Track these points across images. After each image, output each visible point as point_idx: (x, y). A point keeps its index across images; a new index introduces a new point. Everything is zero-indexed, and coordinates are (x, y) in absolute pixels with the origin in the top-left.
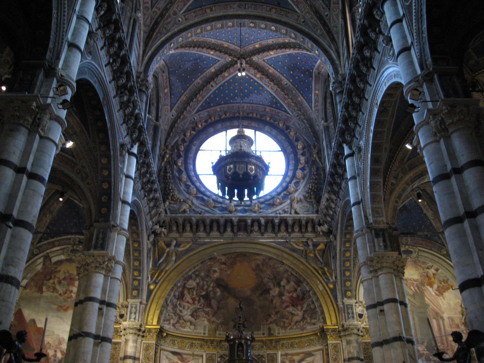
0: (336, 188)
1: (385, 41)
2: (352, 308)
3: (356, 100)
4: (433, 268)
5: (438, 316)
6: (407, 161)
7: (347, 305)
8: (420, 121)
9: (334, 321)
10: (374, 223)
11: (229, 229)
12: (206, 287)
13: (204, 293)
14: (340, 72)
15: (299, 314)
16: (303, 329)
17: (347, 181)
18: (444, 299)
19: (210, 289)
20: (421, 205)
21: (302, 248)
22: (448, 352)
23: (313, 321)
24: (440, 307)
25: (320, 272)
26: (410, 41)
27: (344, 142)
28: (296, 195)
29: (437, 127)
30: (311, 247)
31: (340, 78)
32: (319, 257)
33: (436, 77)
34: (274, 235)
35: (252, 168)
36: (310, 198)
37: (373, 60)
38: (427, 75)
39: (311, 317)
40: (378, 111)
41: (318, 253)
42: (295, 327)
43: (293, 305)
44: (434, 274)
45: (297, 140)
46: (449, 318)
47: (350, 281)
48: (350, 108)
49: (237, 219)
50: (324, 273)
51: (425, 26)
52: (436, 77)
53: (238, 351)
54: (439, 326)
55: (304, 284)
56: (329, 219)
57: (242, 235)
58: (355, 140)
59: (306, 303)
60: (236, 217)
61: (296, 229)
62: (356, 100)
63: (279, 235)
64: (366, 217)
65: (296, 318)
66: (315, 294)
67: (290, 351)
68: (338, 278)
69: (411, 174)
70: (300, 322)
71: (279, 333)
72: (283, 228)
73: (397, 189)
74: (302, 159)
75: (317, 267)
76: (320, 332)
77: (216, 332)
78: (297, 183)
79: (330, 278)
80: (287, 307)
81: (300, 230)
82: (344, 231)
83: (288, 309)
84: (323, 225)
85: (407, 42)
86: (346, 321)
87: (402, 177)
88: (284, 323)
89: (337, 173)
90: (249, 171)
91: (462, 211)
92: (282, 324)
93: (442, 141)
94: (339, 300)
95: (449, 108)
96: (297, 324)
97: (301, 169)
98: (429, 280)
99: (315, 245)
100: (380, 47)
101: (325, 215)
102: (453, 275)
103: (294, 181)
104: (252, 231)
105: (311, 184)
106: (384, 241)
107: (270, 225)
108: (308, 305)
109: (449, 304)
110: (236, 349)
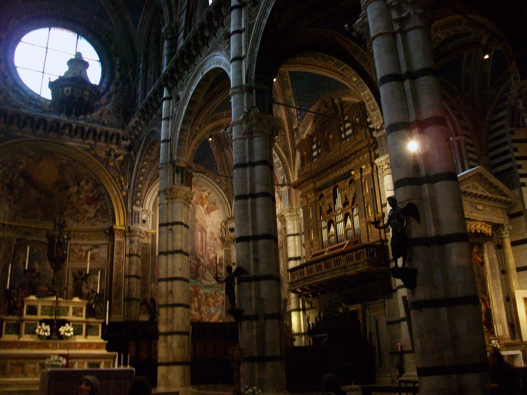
0: (147, 116)
1: (224, 36)
2: (139, 215)
3: (186, 61)
4: (207, 191)
5: (203, 230)
6: (211, 115)
7: (135, 212)
8: (236, 120)
9: (122, 223)
10: (177, 161)
11: (42, 128)
12: (10, 176)
13: (8, 182)
14: (175, 20)
15: (92, 211)
16: (93, 225)
17: (161, 120)
18: (210, 217)
19: (15, 179)
20: (210, 143)
21: (104, 157)
22: (205, 258)
23: (104, 220)
24: (206, 223)
25: (117, 180)
26: (243, 54)
27: (165, 86)
28: (107, 107)
29: (247, 130)
30: (112, 157)
31: (173, 25)
32: (118, 167)
33: (254, 91)
34: (81, 141)
35: (86, 94)
36: (119, 113)
37: (209, 40)
38: (249, 88)
39: (102, 216)
40: (202, 78)
41: (118, 163)
42: (87, 222)
43: (88, 204)
44: (206, 197)
45: (116, 55)
46: (210, 232)
47: (141, 192)
48: (179, 65)
49: (51, 120)
50: (120, 181)
51: (257, 49)
52: (254, 91)
53: (57, 248)
54: (202, 237)
55: (102, 188)
56: (133, 137)
57: (52, 134)
58: (175, 88)
59: (100, 203)
60: (50, 118)
61: (103, 139)
62: (186, 61)
63: (87, 141)
64: (171, 155)
65: (89, 215)
66: (109, 197)
67: (80, 242)
68: (132, 187)
69: (211, 126)
70: (92, 218)
71: (72, 225)
72: (91, 135)
73: (199, 136)
74: (117, 75)
75: (115, 176)
76: (109, 231)
77: (15, 218)
78: (109, 97)
79: (124, 187)
80: (82, 204)
81: (106, 141)
82: (145, 152)
83: (83, 206)
84: (127, 140)
85: (241, 52)
86: (132, 224)
87: (204, 127)
88: (78, 217)
89: (152, 106)
90: (84, 97)
91: (248, 192)
92: (76, 218)
93: (247, 141)
94: (129, 206)
95: (257, 120)
96: (89, 220)
97: (115, 84)
98: (202, 200)
99: (117, 156)
100: (218, 35)
101: (130, 133)
102: (220, 199)
103: (107, 94)
104: (62, 134)
105: (121, 101)
106: (182, 177)
107: (79, 131)
108: (101, 206)
109: (213, 222)
110: (55, 246)
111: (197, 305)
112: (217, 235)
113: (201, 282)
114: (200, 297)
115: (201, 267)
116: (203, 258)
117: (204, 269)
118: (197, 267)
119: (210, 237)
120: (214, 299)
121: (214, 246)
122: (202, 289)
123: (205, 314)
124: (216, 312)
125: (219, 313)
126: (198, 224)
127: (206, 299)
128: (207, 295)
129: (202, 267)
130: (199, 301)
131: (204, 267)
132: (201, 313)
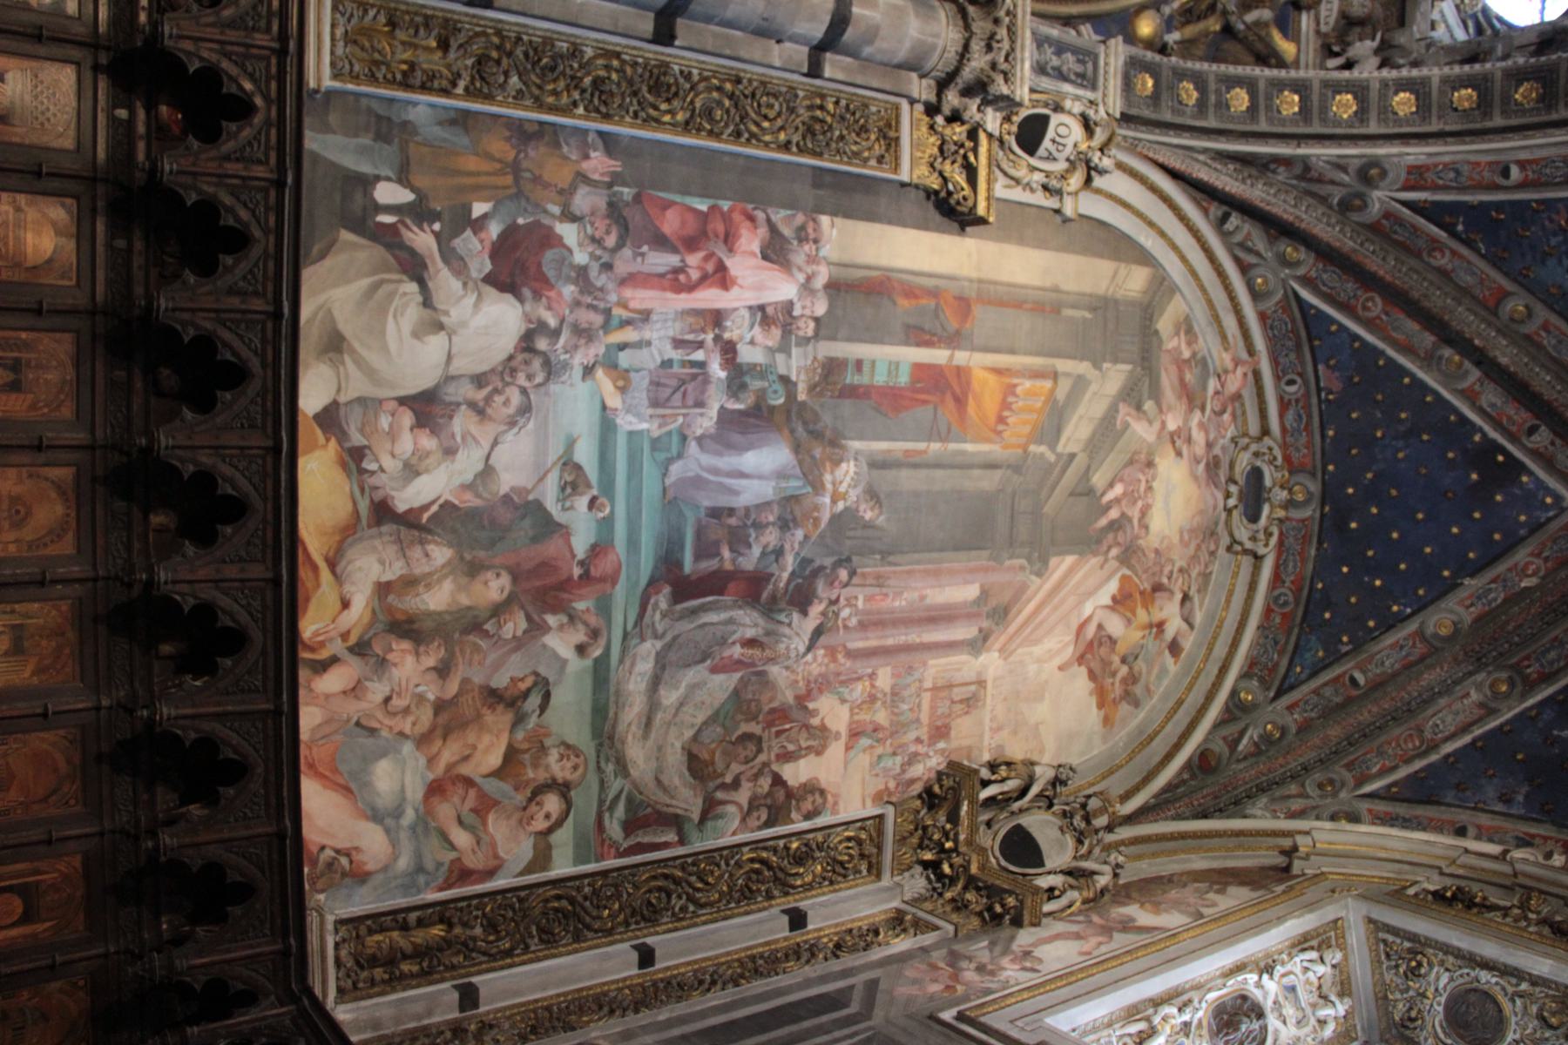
18: (1061, 668)
102: (1156, 733)
109: (1038, 696)
111: (437, 599)
112: (966, 742)
113: (639, 628)
114: (515, 625)
115: (749, 622)
116: (818, 632)
117: (737, 651)
118: (753, 588)
119: (950, 686)
120: (498, 774)
121: (898, 728)
122: (581, 649)
123: (355, 690)
124: (376, 816)
125: (372, 843)
126: (1020, 577)
127: (494, 697)
128: (534, 701)
129: (750, 633)
130: (471, 624)
131: (757, 652)
132: (360, 649)
